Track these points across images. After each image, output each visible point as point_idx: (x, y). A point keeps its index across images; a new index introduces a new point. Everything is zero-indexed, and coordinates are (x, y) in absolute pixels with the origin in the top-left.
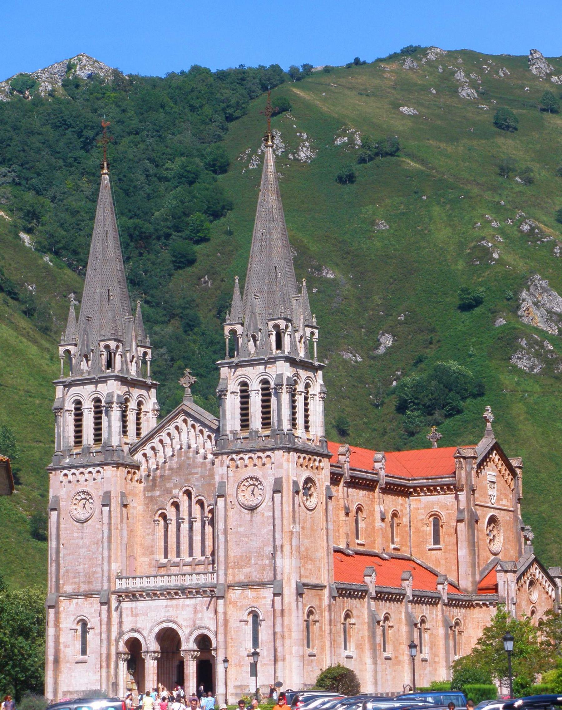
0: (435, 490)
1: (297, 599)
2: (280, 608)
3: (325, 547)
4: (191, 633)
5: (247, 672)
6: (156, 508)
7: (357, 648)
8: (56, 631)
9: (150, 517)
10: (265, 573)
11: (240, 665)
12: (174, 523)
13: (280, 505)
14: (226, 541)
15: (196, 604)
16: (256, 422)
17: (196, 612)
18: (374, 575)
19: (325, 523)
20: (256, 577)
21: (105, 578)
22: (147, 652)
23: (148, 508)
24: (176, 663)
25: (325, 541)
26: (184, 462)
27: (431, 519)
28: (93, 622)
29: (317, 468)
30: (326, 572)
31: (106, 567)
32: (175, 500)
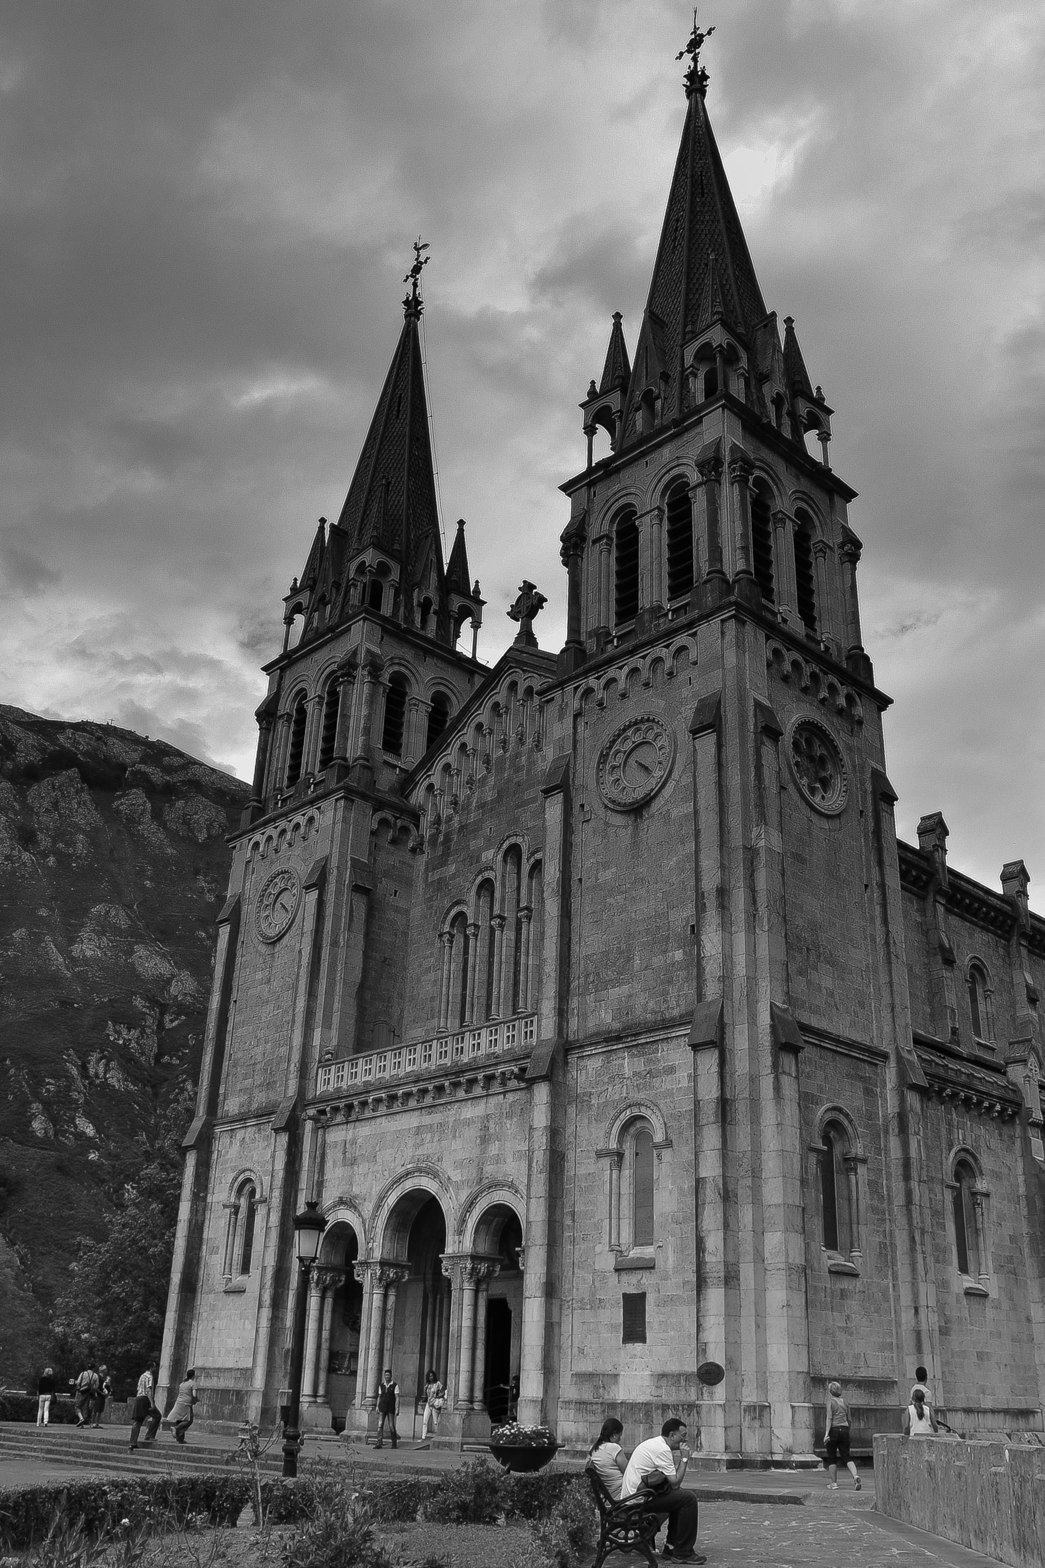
2: (715, 1093)
3: (880, 940)
4: (471, 1205)
5: (613, 1327)
7: (999, 1269)
9: (435, 929)
10: (673, 991)
11: (596, 1304)
12: (484, 934)
14: (566, 914)
15: (488, 1117)
16: (653, 588)
17: (485, 1139)
18: (1032, 1060)
19: (875, 871)
20: (645, 1007)
22: (366, 1264)
25: (878, 921)
26: (509, 780)
29: (840, 712)
30: (886, 1014)
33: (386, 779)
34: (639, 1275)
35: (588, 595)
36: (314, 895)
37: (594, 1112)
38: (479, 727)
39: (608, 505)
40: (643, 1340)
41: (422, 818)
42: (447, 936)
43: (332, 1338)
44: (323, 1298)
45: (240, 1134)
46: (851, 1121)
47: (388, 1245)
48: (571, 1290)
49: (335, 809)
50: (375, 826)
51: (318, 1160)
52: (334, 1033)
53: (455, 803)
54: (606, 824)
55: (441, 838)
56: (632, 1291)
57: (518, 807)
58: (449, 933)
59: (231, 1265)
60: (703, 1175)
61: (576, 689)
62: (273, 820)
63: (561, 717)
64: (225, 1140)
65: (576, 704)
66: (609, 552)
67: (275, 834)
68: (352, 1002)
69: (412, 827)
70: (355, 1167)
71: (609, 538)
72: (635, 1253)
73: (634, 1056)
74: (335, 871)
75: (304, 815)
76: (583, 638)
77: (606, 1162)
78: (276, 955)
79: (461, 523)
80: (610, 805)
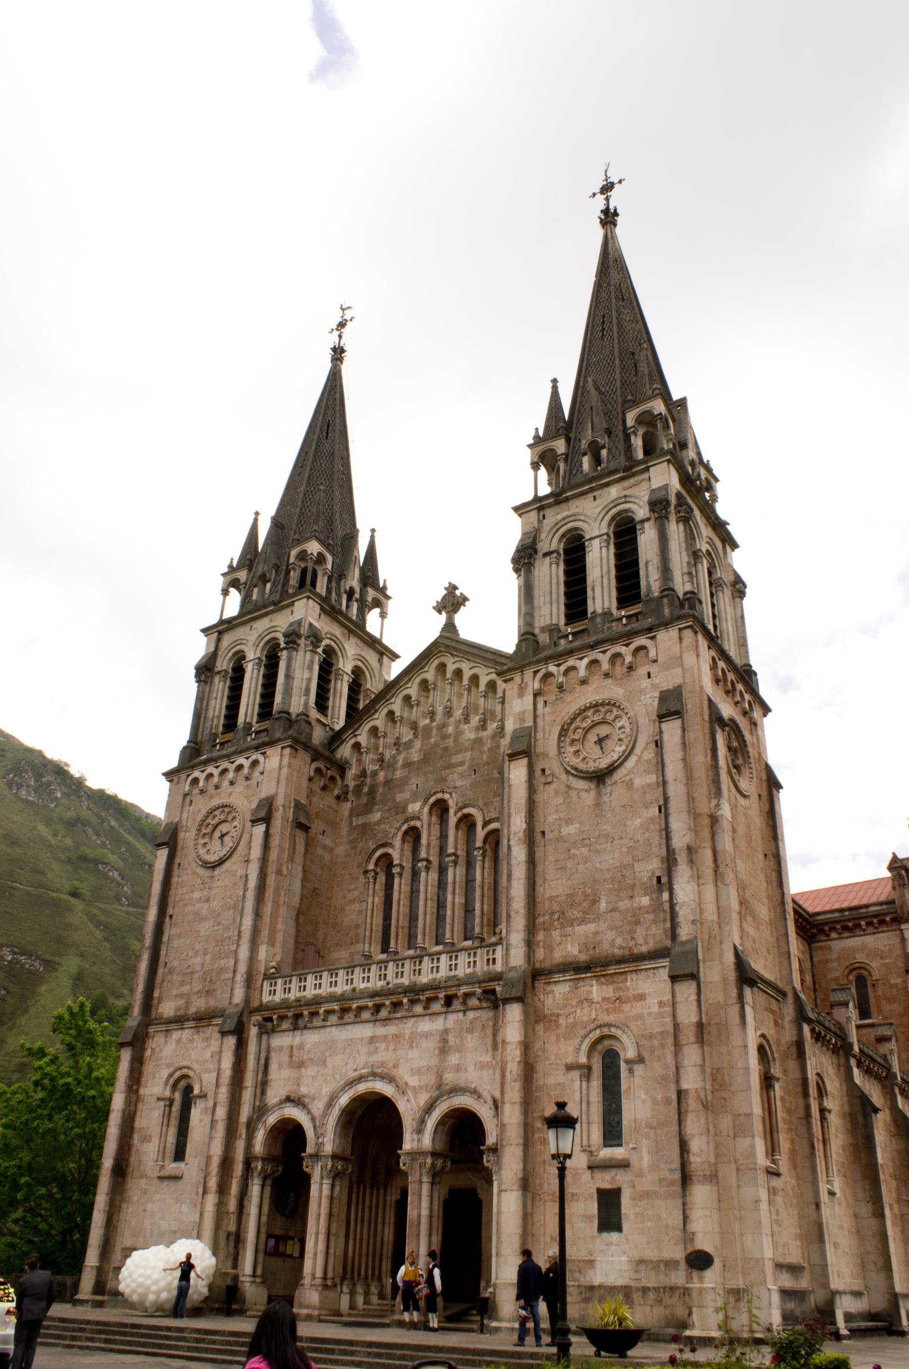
0: (859, 925)
1: (741, 997)
2: (694, 1019)
4: (429, 1108)
5: (588, 1218)
6: (372, 845)
8: (128, 1102)
10: (640, 932)
12: (407, 873)
13: (679, 747)
14: (532, 861)
15: (446, 1031)
17: (444, 1049)
21: (240, 978)
22: (316, 1156)
23: (354, 848)
24: (393, 1196)
26: (436, 745)
27: (852, 977)
28: (203, 1081)
31: (244, 953)
32: (412, 823)
33: (318, 736)
34: (613, 1172)
35: (540, 598)
36: (261, 828)
37: (562, 1030)
38: (407, 699)
39: (557, 527)
40: (619, 1229)
41: (347, 771)
42: (372, 874)
43: (269, 1224)
44: (263, 1186)
45: (176, 1035)
46: (770, 1046)
47: (337, 1140)
48: (541, 1185)
49: (282, 756)
50: (312, 773)
51: (262, 1061)
52: (278, 950)
53: (381, 760)
54: (568, 787)
55: (366, 789)
56: (606, 1186)
57: (445, 768)
58: (374, 870)
59: (164, 1153)
60: (684, 1086)
61: (536, 673)
62: (215, 760)
63: (521, 694)
64: (159, 1039)
65: (537, 685)
66: (558, 564)
67: (216, 772)
68: (292, 924)
69: (338, 778)
70: (303, 1070)
71: (559, 554)
72: (606, 1153)
73: (602, 983)
74: (281, 809)
75: (247, 758)
76: (537, 631)
77: (576, 1074)
78: (216, 878)
79: (373, 531)
80: (573, 771)
